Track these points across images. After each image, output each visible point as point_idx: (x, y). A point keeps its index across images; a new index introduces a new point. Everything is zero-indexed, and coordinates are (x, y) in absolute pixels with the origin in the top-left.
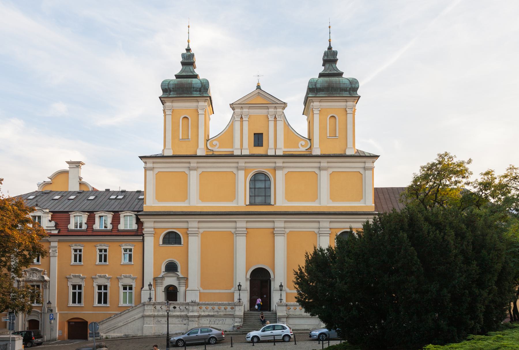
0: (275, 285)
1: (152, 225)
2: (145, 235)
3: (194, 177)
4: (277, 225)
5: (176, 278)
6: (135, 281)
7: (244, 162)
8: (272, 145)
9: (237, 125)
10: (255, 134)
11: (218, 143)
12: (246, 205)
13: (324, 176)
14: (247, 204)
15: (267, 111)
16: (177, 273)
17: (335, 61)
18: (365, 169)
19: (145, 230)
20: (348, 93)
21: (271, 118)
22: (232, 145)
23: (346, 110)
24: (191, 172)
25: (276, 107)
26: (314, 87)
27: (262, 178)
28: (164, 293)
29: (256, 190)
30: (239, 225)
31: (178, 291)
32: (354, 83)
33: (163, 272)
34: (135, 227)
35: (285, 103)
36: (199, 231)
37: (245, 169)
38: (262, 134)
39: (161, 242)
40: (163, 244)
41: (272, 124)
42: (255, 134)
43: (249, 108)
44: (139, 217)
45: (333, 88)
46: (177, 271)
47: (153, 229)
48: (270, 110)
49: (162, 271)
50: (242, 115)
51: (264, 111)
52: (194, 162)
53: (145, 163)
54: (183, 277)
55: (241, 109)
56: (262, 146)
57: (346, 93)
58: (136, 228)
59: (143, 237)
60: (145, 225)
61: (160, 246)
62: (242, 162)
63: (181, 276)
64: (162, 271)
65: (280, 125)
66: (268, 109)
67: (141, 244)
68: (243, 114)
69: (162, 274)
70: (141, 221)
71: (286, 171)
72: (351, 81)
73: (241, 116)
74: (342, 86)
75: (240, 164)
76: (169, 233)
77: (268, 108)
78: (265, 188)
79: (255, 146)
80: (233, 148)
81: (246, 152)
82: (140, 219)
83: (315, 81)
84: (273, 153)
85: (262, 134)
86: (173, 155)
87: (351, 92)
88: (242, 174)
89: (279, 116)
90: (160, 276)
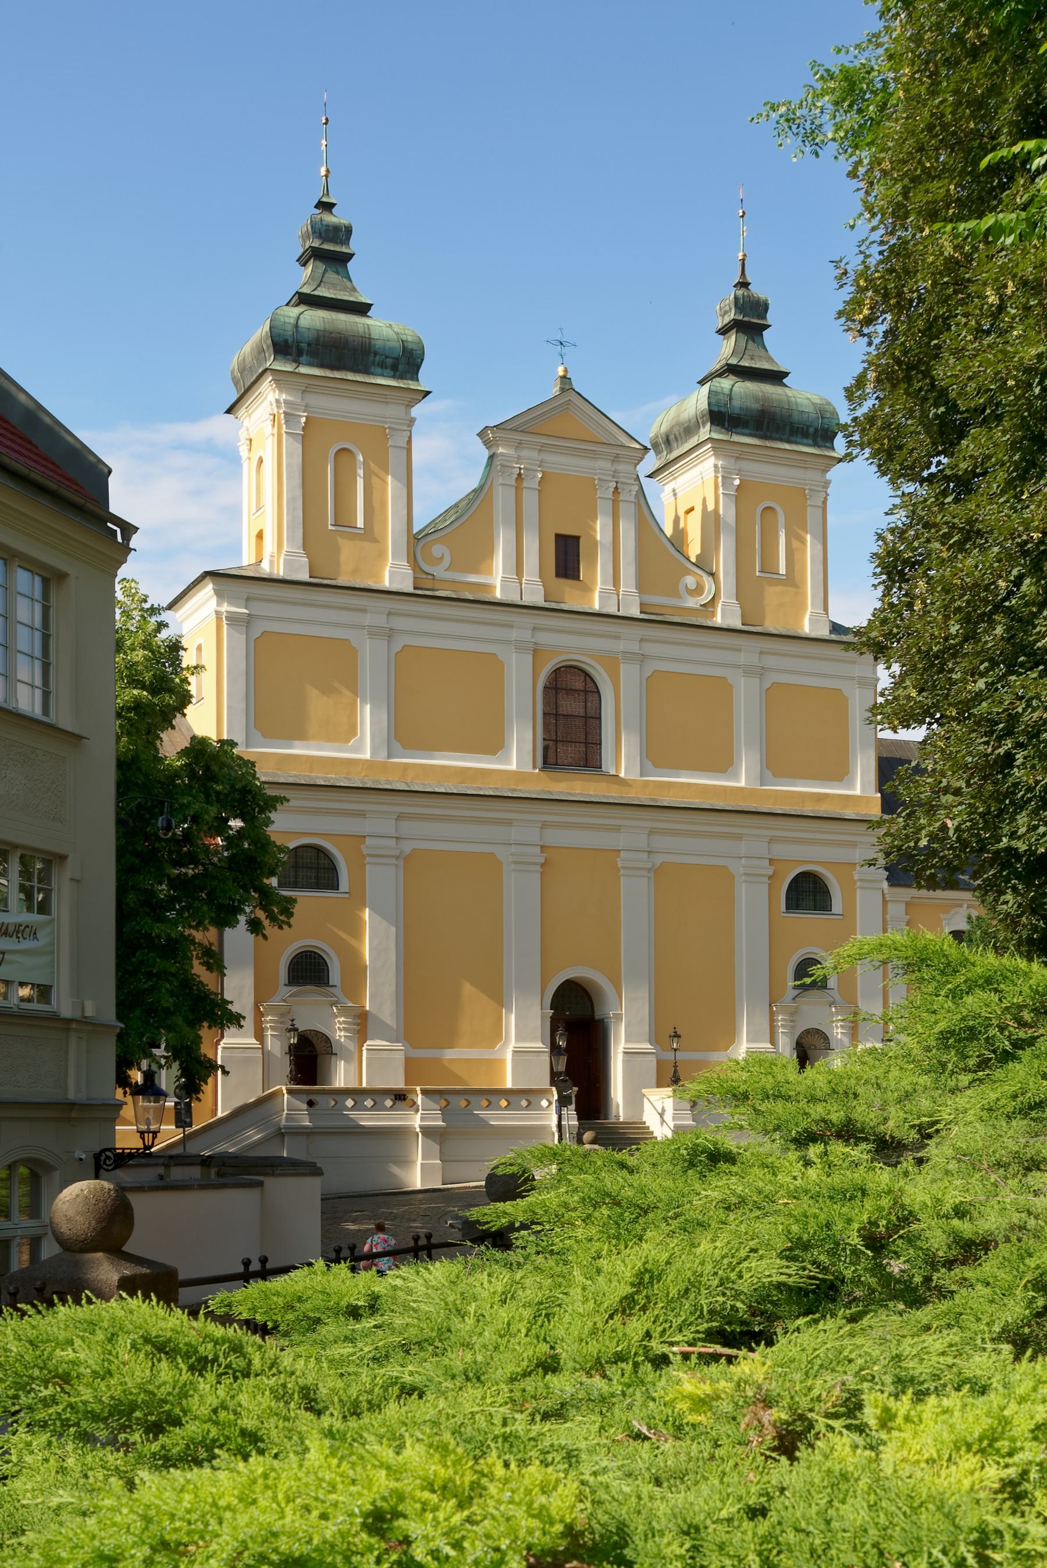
10: (558, 537)
20: (810, 442)
29: (561, 722)
38: (577, 539)
42: (558, 537)
57: (805, 441)
62: (522, 628)
74: (796, 417)
78: (586, 717)
81: (534, 595)
85: (577, 539)
87: (819, 439)
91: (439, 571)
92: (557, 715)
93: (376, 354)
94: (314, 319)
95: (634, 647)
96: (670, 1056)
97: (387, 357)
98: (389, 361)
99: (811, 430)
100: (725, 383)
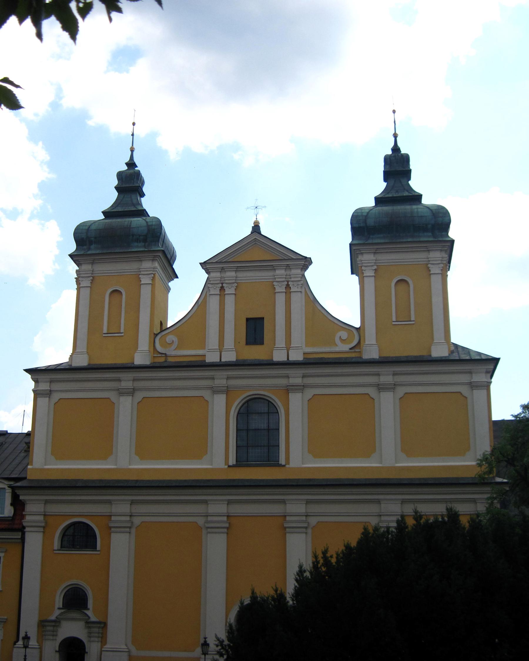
2: (27, 529)
6: (3, 627)
7: (226, 376)
8: (280, 341)
9: (214, 303)
10: (248, 320)
11: (175, 339)
12: (229, 466)
14: (231, 463)
15: (271, 273)
16: (86, 612)
17: (407, 174)
19: (28, 518)
20: (430, 234)
21: (280, 288)
22: (202, 344)
23: (428, 268)
24: (122, 399)
25: (289, 266)
26: (362, 225)
28: (57, 655)
31: (86, 651)
32: (441, 215)
33: (59, 608)
34: (8, 511)
35: (306, 258)
36: (132, 523)
37: (227, 391)
38: (263, 319)
39: (56, 544)
40: (61, 547)
41: (280, 299)
42: (248, 320)
43: (237, 269)
44: (18, 492)
46: (86, 608)
47: (41, 518)
48: (278, 272)
49: (57, 606)
50: (222, 284)
51: (267, 275)
53: (36, 381)
54: (98, 620)
55: (221, 272)
56: (262, 343)
58: (12, 515)
59: (23, 534)
60: (29, 508)
61: (55, 552)
63: (93, 619)
64: (57, 606)
65: (297, 300)
66: (275, 269)
68: (226, 282)
69: (57, 612)
70: (21, 500)
72: (434, 211)
73: (221, 285)
77: (273, 268)
79: (248, 343)
80: (204, 348)
81: (230, 357)
82: (18, 496)
83: (365, 214)
84: (283, 358)
85: (263, 319)
86: (89, 365)
88: (220, 400)
89: (295, 284)
90: (53, 618)
91: (171, 351)
92: (248, 430)
93: (133, 235)
95: (298, 381)
97: (140, 236)
98: (142, 237)
99: (429, 226)
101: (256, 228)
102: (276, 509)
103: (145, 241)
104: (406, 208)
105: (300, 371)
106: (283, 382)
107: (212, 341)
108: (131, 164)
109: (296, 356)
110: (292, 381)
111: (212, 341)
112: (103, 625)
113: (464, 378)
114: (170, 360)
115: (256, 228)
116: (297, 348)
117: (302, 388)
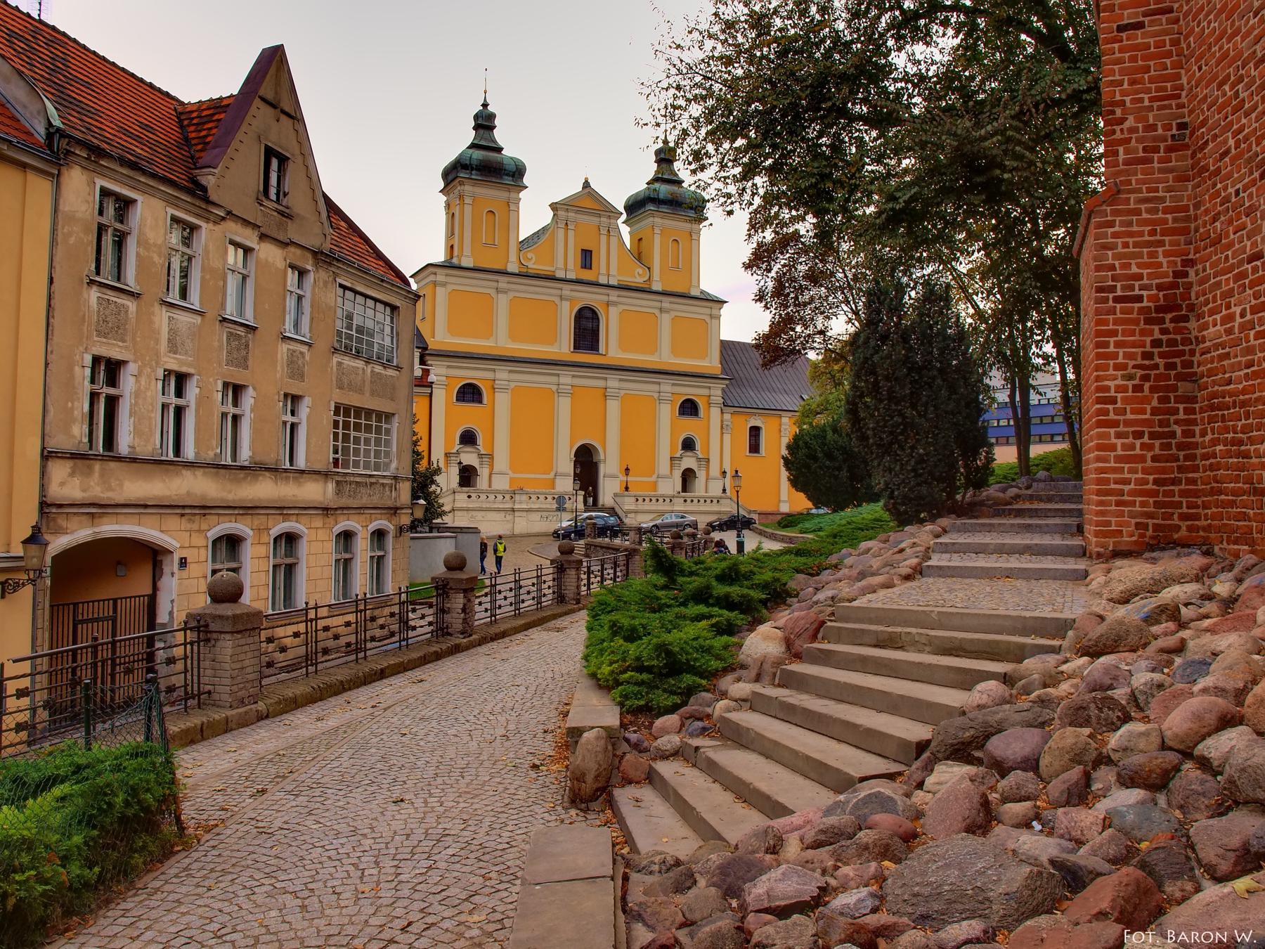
0: (602, 470)
1: (443, 371)
3: (503, 302)
4: (611, 383)
5: (475, 455)
8: (603, 270)
9: (561, 233)
13: (666, 319)
18: (711, 316)
21: (604, 231)
22: (552, 260)
27: (589, 315)
30: (562, 380)
37: (570, 299)
41: (604, 239)
43: (577, 212)
45: (677, 202)
51: (595, 220)
52: (503, 282)
62: (567, 290)
63: (482, 452)
65: (614, 240)
67: (427, 401)
69: (457, 447)
71: (622, 307)
75: (564, 292)
76: (464, 386)
81: (571, 276)
84: (605, 282)
88: (566, 305)
90: (454, 451)
94: (478, 155)
96: (625, 479)
100: (657, 185)
101: (586, 185)
102: (601, 383)
103: (513, 176)
104: (675, 188)
105: (617, 292)
106: (605, 298)
107: (560, 263)
108: (485, 105)
109: (613, 282)
110: (611, 298)
111: (560, 263)
112: (491, 456)
113: (708, 311)
114: (530, 271)
115: (586, 185)
116: (614, 276)
117: (615, 304)
